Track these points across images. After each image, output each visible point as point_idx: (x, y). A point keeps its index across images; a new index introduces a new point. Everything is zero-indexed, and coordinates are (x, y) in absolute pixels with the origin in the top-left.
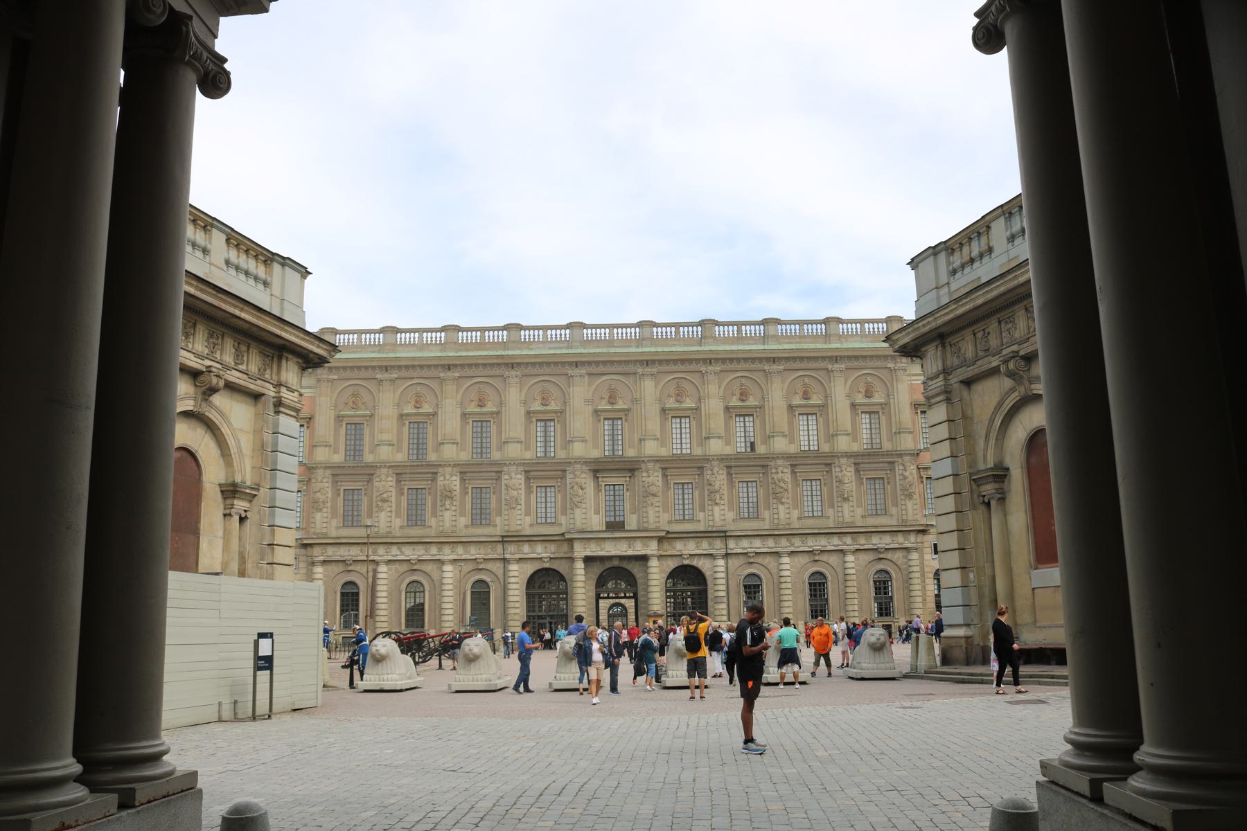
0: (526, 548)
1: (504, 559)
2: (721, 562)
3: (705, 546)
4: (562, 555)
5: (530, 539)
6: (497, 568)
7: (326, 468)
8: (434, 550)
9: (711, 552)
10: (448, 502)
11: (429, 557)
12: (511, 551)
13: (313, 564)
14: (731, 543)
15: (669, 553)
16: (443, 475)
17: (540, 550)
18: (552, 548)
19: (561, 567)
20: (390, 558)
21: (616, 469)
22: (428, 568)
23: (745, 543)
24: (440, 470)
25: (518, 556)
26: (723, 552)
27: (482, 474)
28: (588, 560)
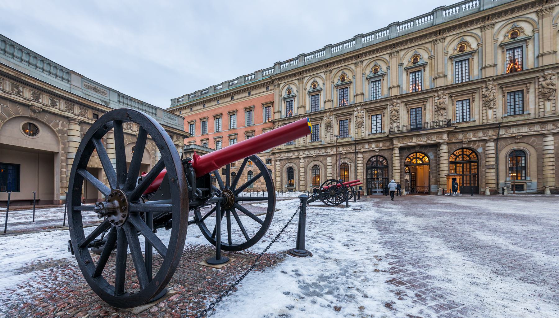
0: (367, 146)
1: (356, 153)
2: (493, 144)
3: (480, 135)
4: (386, 148)
5: (369, 141)
6: (353, 156)
7: (279, 121)
8: (323, 151)
9: (484, 138)
10: (329, 128)
11: (321, 154)
12: (359, 148)
13: (276, 161)
14: (502, 132)
15: (454, 141)
16: (327, 116)
17: (373, 146)
18: (381, 144)
19: (386, 154)
20: (305, 156)
21: (415, 100)
22: (321, 159)
23: (514, 130)
24: (325, 114)
25: (362, 150)
26: (495, 137)
27: (343, 113)
28: (401, 149)
